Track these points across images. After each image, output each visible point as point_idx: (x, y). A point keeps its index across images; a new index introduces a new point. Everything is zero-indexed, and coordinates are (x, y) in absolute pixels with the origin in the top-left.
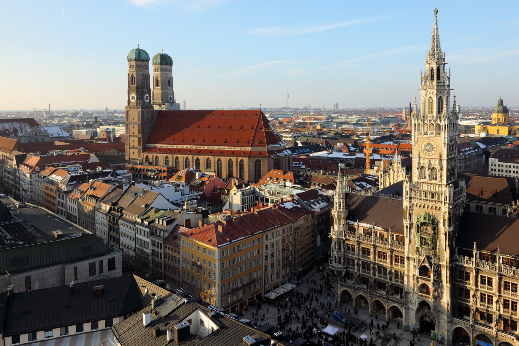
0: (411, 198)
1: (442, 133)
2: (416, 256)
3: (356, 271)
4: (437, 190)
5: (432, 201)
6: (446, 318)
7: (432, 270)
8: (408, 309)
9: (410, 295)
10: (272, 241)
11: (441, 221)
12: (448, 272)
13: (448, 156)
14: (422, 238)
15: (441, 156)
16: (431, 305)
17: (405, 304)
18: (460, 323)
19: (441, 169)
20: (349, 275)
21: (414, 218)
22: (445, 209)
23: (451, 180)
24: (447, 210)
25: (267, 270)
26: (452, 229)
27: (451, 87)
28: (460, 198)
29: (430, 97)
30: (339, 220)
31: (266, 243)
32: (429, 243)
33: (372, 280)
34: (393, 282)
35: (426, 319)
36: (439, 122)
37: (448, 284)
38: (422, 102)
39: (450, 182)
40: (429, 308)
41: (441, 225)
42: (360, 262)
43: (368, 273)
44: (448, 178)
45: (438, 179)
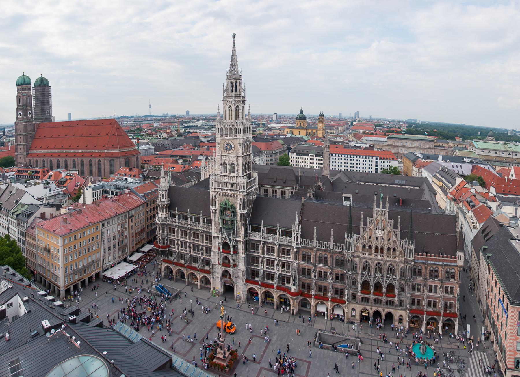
2: (220, 236)
3: (176, 250)
4: (235, 181)
5: (231, 190)
9: (216, 266)
10: (109, 228)
11: (238, 206)
12: (243, 245)
13: (243, 154)
14: (223, 220)
19: (238, 165)
21: (217, 203)
23: (246, 172)
24: (242, 197)
25: (105, 252)
27: (246, 99)
28: (253, 186)
29: (230, 106)
31: (103, 230)
32: (228, 225)
33: (188, 257)
34: (204, 257)
36: (236, 126)
39: (245, 174)
42: (179, 242)
43: (185, 250)
45: (236, 172)
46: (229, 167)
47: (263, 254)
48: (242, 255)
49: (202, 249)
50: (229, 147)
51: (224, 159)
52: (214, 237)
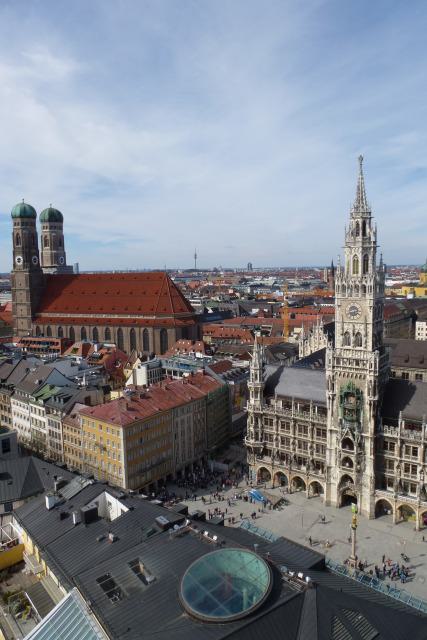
0: (333, 367)
1: (367, 296)
2: (338, 429)
6: (368, 490)
7: (355, 442)
8: (329, 485)
11: (366, 391)
13: (373, 320)
14: (345, 409)
15: (366, 320)
16: (354, 478)
17: (327, 480)
18: (382, 495)
19: (366, 335)
20: (266, 452)
21: (336, 387)
22: (370, 377)
24: (372, 379)
26: (376, 398)
27: (378, 244)
30: (256, 393)
32: (353, 415)
34: (315, 457)
35: (349, 493)
36: (364, 283)
37: (372, 457)
38: (346, 261)
40: (352, 482)
41: (366, 395)
44: (374, 344)
46: (352, 338)
47: (401, 456)
48: (369, 457)
49: (311, 447)
50: (354, 312)
51: (346, 327)
52: (331, 431)
